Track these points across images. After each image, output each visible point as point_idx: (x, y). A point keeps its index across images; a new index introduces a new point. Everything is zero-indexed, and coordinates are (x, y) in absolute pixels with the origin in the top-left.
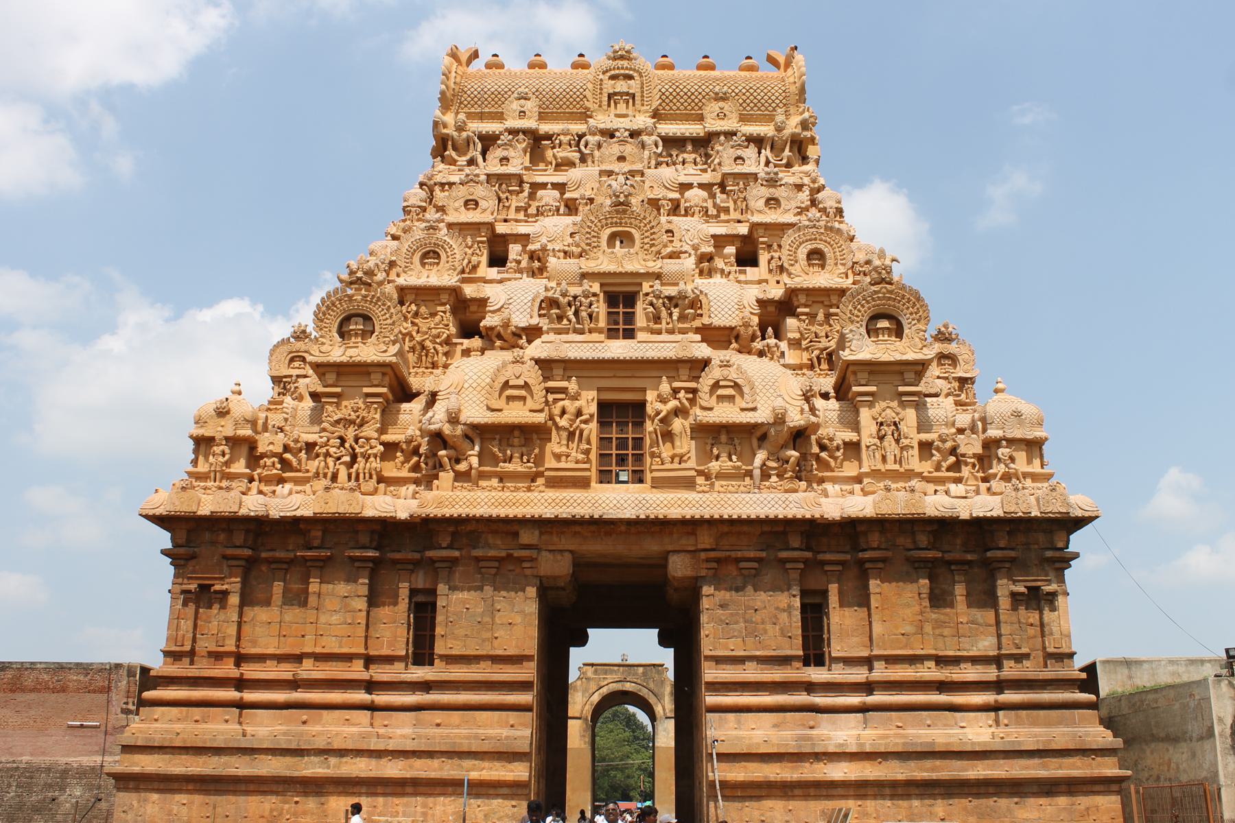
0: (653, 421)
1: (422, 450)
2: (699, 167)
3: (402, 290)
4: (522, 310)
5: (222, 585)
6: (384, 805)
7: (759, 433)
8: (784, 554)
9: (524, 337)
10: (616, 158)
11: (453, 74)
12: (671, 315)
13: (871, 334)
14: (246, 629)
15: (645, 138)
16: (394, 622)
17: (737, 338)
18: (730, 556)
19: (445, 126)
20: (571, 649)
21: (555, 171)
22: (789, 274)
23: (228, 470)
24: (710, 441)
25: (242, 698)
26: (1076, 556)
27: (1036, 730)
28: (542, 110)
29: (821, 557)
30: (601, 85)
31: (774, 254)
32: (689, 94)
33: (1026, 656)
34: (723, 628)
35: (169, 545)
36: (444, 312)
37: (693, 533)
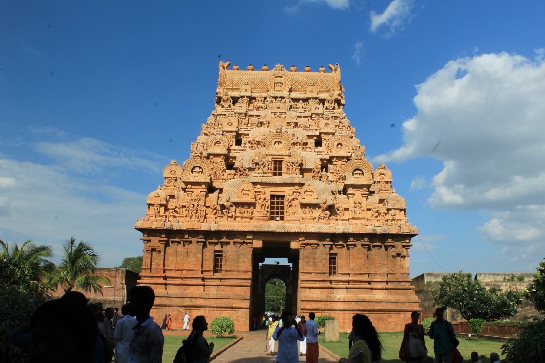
3: (209, 155)
6: (208, 313)
7: (318, 206)
11: (223, 75)
13: (354, 175)
14: (166, 262)
16: (210, 260)
17: (314, 172)
19: (220, 94)
21: (257, 110)
27: (396, 296)
28: (252, 88)
29: (336, 243)
33: (396, 274)
36: (222, 162)
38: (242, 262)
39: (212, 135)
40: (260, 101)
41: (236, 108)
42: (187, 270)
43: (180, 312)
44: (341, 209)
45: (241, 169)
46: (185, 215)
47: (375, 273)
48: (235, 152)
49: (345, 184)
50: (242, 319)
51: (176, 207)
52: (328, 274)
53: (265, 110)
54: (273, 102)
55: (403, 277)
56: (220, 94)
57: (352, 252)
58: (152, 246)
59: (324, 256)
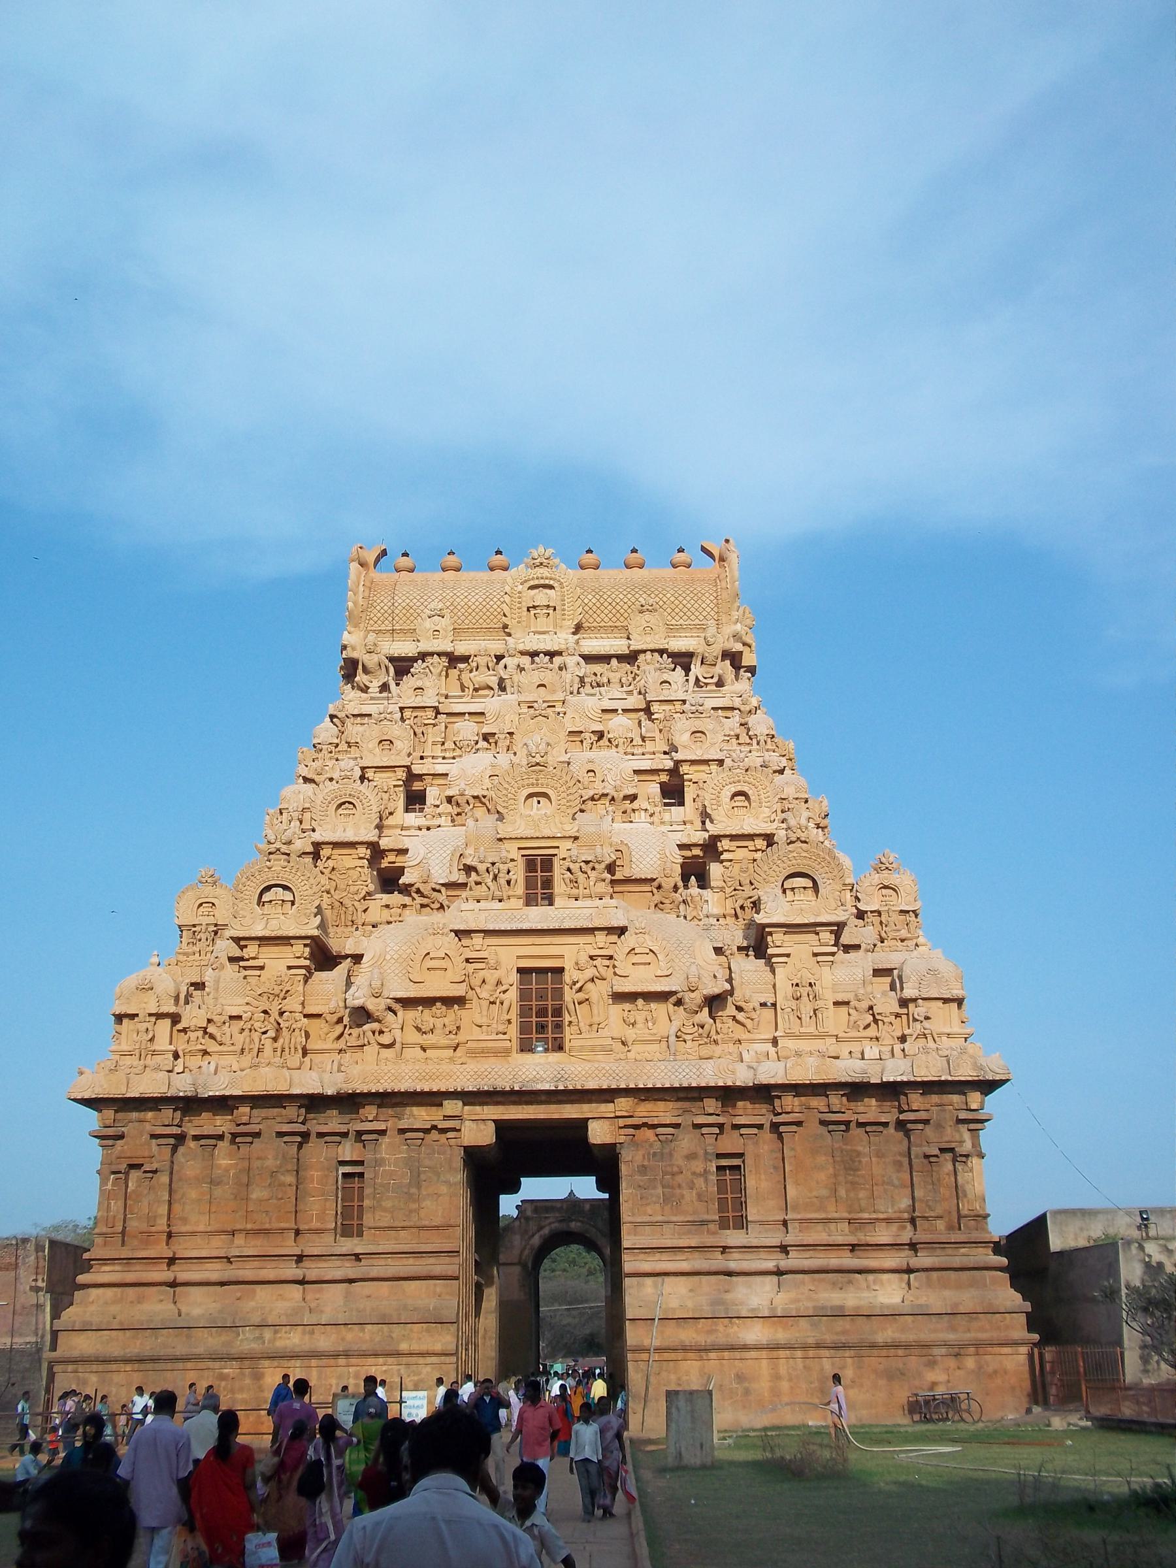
2: (625, 689)
3: (317, 846)
4: (441, 865)
6: (319, 1378)
8: (700, 1120)
11: (361, 588)
13: (787, 891)
14: (176, 1207)
17: (659, 887)
19: (354, 649)
20: (502, 1197)
23: (152, 1048)
27: (947, 1293)
38: (428, 1195)
39: (328, 783)
40: (483, 669)
41: (405, 693)
44: (751, 1005)
45: (422, 889)
46: (238, 1048)
47: (874, 1216)
48: (404, 833)
53: (499, 696)
54: (522, 669)
55: (966, 1226)
56: (354, 649)
57: (793, 1149)
58: (128, 1155)
59: (698, 1166)
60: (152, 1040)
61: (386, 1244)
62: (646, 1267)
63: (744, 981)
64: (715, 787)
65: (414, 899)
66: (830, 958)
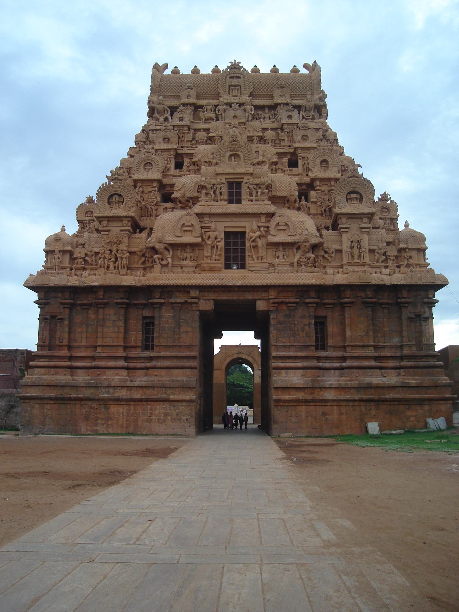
0: (249, 241)
1: (147, 255)
3: (135, 181)
5: (61, 316)
7: (296, 246)
8: (308, 300)
9: (191, 201)
10: (232, 117)
12: (257, 192)
13: (348, 200)
15: (246, 107)
17: (288, 201)
18: (283, 301)
19: (153, 103)
21: (205, 123)
22: (312, 172)
23: (61, 266)
24: (275, 250)
25: (72, 364)
26: (437, 301)
27: (417, 378)
28: (198, 94)
29: (324, 301)
30: (225, 81)
31: (305, 162)
32: (267, 85)
34: (280, 333)
35: (37, 299)
37: (267, 291)
38: (183, 332)
42: (102, 346)
43: (92, 408)
44: (331, 251)
45: (181, 200)
49: (336, 213)
50: (184, 418)
51: (86, 255)
52: (313, 348)
59: (307, 321)
60: (60, 262)
61: (164, 353)
62: (282, 364)
63: (328, 240)
64: (313, 158)
65: (178, 205)
66: (368, 230)
